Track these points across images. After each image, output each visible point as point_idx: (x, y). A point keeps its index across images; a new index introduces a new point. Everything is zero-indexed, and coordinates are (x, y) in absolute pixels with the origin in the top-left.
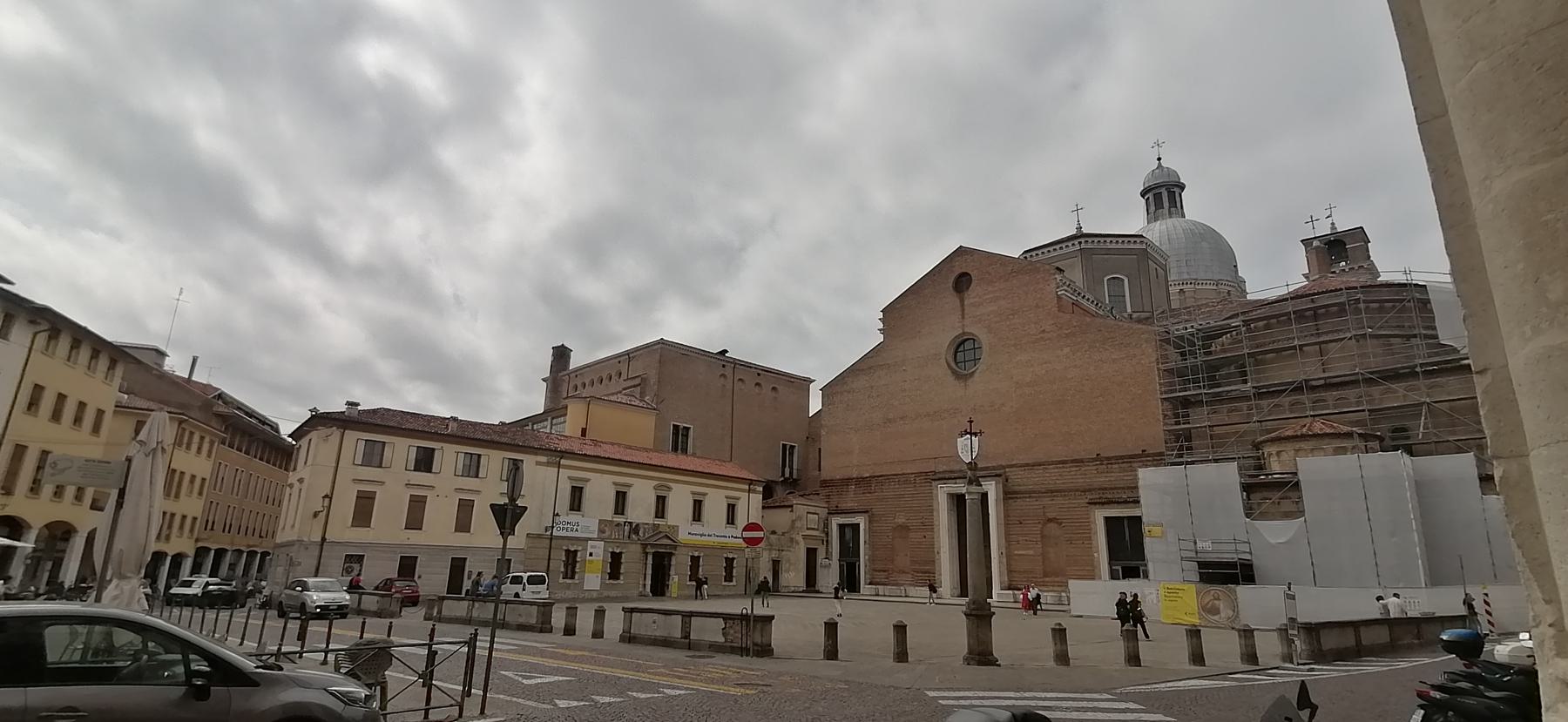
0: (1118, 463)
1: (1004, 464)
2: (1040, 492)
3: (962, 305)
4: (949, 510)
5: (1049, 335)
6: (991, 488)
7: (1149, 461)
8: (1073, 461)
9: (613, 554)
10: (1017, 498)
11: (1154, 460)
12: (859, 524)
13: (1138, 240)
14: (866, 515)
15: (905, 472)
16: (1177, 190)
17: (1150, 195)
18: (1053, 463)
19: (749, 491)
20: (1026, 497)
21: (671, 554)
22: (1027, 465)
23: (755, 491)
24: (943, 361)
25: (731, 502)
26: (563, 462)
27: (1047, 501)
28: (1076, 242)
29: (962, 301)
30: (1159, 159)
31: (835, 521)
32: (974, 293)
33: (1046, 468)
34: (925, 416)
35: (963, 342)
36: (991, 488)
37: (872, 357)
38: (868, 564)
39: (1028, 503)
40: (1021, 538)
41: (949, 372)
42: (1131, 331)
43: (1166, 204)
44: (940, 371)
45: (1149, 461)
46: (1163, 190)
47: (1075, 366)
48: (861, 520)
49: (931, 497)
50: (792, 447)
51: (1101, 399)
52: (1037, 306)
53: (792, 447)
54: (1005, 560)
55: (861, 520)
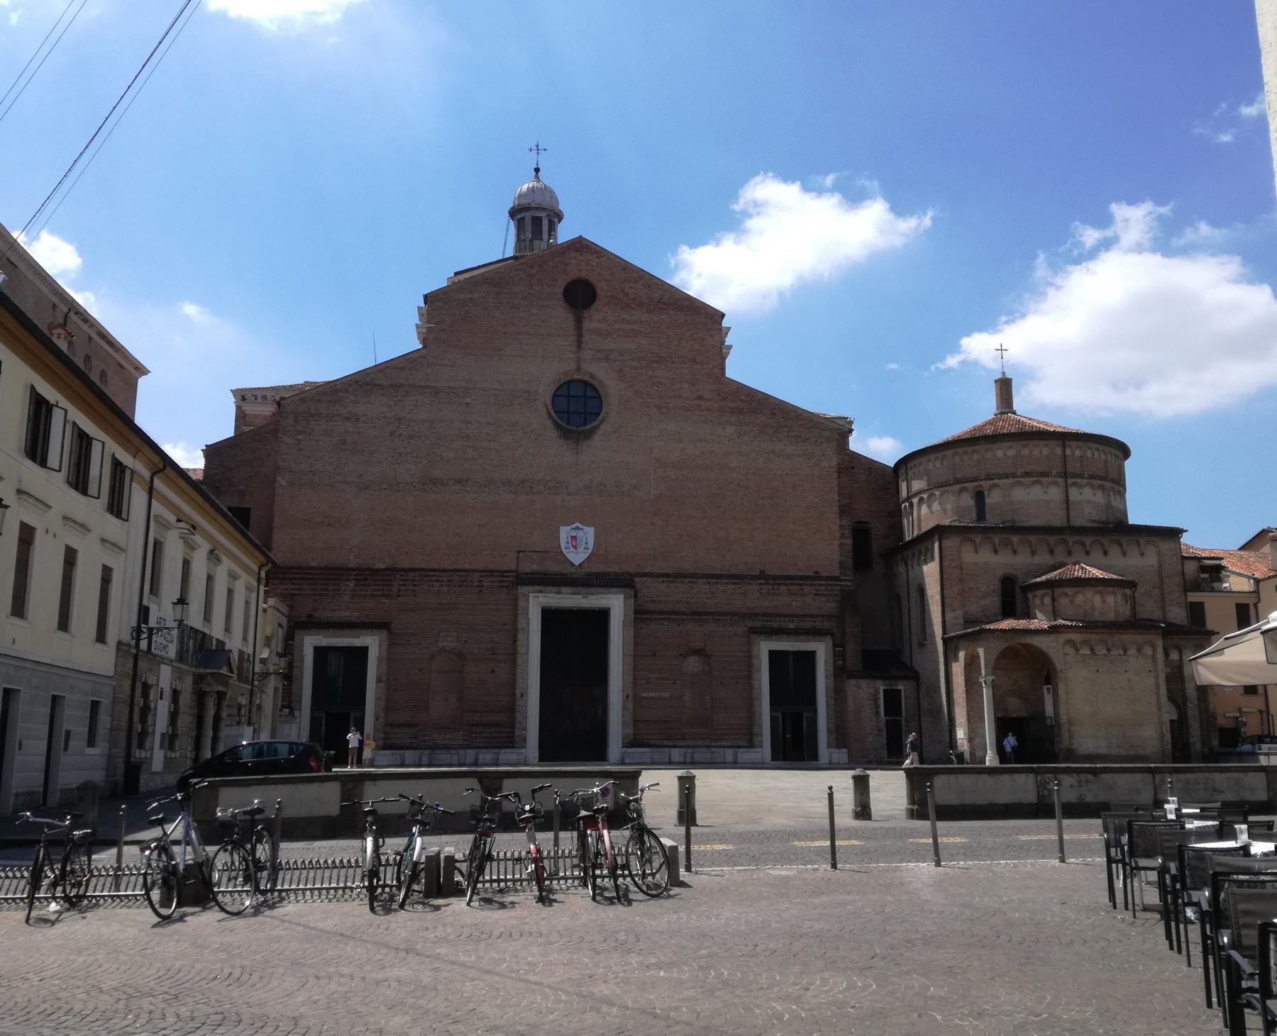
0: (787, 584)
1: (631, 570)
2: (683, 613)
5: (708, 404)
7: (823, 585)
10: (650, 619)
11: (828, 585)
12: (367, 648)
14: (384, 634)
15: (460, 567)
18: (703, 576)
20: (664, 619)
22: (668, 575)
29: (579, 321)
31: (310, 642)
32: (596, 318)
33: (694, 583)
34: (503, 483)
36: (616, 604)
37: (402, 369)
38: (382, 715)
41: (549, 423)
42: (811, 424)
44: (538, 418)
45: (823, 585)
48: (373, 643)
49: (516, 611)
52: (694, 361)
54: (630, 705)
55: (373, 643)
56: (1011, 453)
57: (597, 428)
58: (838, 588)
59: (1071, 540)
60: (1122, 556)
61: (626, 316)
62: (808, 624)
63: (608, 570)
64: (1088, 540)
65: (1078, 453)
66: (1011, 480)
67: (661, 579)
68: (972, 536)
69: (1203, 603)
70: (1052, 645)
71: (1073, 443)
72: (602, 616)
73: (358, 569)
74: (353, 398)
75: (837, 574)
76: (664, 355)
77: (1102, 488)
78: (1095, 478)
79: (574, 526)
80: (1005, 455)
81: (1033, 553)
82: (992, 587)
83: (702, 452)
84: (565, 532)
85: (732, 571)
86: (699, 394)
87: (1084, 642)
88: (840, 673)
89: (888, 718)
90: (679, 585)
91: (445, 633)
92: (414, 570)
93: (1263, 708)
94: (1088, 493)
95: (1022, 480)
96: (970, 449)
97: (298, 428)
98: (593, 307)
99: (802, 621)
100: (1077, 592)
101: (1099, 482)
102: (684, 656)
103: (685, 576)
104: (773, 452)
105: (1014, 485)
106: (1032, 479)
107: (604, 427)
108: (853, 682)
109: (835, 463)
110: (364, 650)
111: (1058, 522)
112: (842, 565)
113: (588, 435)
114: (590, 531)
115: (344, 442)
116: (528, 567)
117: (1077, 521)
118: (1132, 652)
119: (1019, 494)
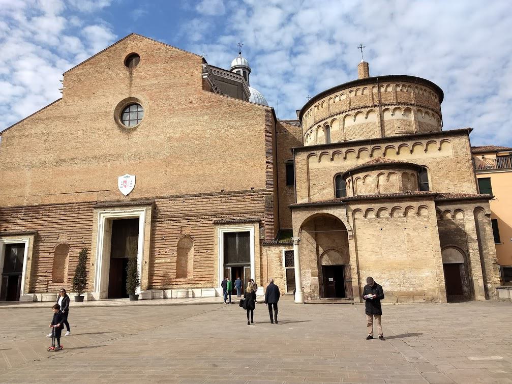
1: (154, 196)
3: (131, 77)
4: (106, 231)
6: (143, 215)
8: (205, 195)
11: (259, 194)
12: (24, 244)
16: (247, 72)
22: (172, 197)
27: (184, 223)
29: (131, 73)
32: (141, 69)
35: (129, 106)
36: (143, 215)
39: (170, 224)
40: (161, 251)
42: (250, 108)
44: (110, 123)
51: (227, 153)
52: (188, 84)
57: (139, 125)
58: (264, 195)
60: (425, 152)
61: (154, 67)
62: (246, 217)
63: (141, 197)
64: (396, 145)
66: (344, 114)
67: (168, 199)
68: (315, 152)
69: (489, 179)
70: (342, 213)
72: (135, 221)
74: (30, 126)
75: (264, 188)
76: (172, 84)
78: (402, 104)
79: (125, 176)
80: (340, 100)
82: (329, 182)
83: (191, 131)
84: (121, 179)
86: (190, 101)
87: (368, 210)
88: (263, 243)
89: (287, 268)
90: (178, 202)
91: (61, 235)
92: (49, 205)
95: (350, 113)
97: (8, 143)
98: (138, 66)
99: (243, 216)
100: (366, 176)
104: (229, 126)
105: (345, 117)
106: (356, 111)
108: (267, 248)
109: (263, 128)
112: (267, 183)
113: (134, 129)
114: (133, 178)
117: (389, 134)
118: (411, 213)
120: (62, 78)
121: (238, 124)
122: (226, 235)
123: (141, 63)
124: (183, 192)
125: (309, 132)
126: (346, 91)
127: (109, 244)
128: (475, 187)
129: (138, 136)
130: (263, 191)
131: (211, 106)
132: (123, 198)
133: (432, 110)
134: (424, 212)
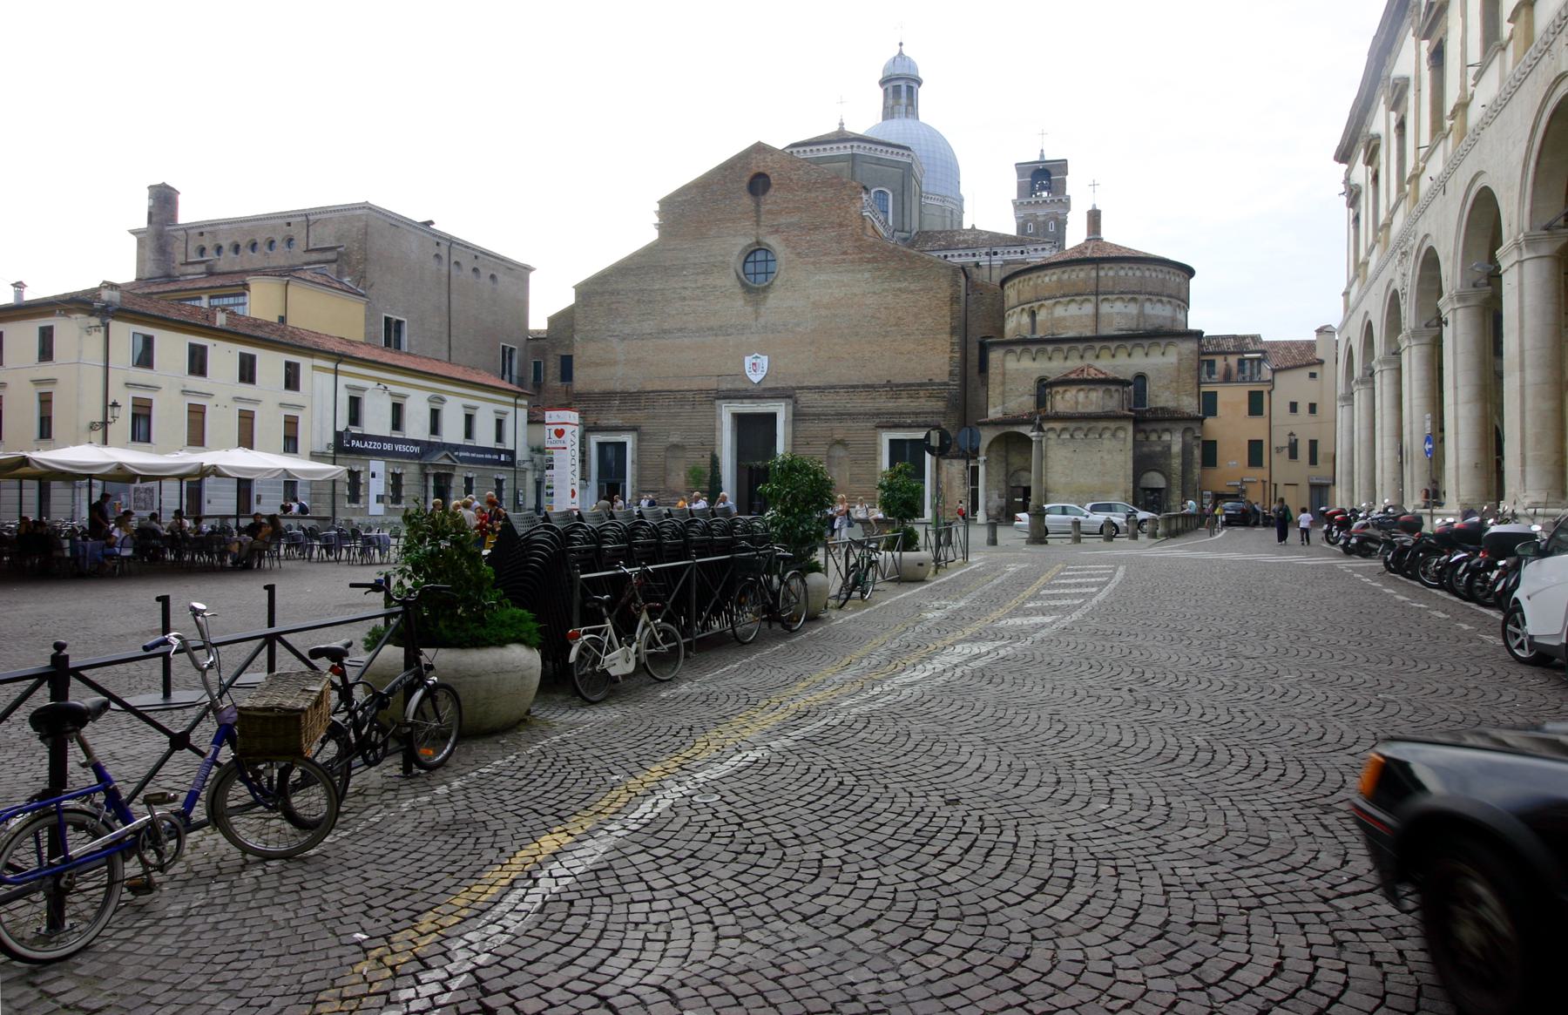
3: (758, 211)
6: (781, 411)
9: (394, 474)
13: (906, 153)
14: (635, 434)
16: (914, 85)
17: (889, 86)
19: (516, 405)
21: (450, 476)
22: (818, 388)
23: (521, 406)
24: (732, 270)
25: (500, 416)
26: (341, 367)
28: (848, 145)
29: (758, 205)
30: (901, 44)
31: (594, 440)
32: (771, 199)
35: (754, 252)
36: (781, 411)
43: (904, 100)
44: (728, 281)
46: (902, 83)
47: (875, 293)
48: (629, 439)
49: (715, 417)
50: (512, 350)
53: (512, 350)
55: (629, 439)
56: (1055, 278)
57: (772, 283)
59: (1098, 345)
62: (921, 420)
64: (1113, 345)
65: (1111, 273)
66: (1053, 301)
68: (1014, 348)
71: (1107, 266)
73: (622, 392)
77: (1134, 300)
81: (1066, 358)
84: (748, 361)
85: (868, 382)
87: (1064, 429)
93: (1266, 478)
94: (1119, 306)
96: (1027, 277)
101: (1130, 296)
102: (831, 446)
103: (833, 387)
107: (777, 282)
110: (624, 444)
111: (1088, 333)
112: (951, 373)
113: (765, 289)
114: (765, 359)
115: (611, 309)
116: (725, 386)
118: (1107, 435)
119: (1060, 311)
120: (657, 207)
121: (912, 287)
122: (892, 442)
123: (771, 191)
124: (834, 381)
125: (1011, 312)
126: (1058, 271)
127: (735, 447)
128: (1196, 402)
129: (773, 300)
130: (945, 384)
131: (874, 260)
132: (751, 387)
133: (1169, 296)
134: (1121, 434)
